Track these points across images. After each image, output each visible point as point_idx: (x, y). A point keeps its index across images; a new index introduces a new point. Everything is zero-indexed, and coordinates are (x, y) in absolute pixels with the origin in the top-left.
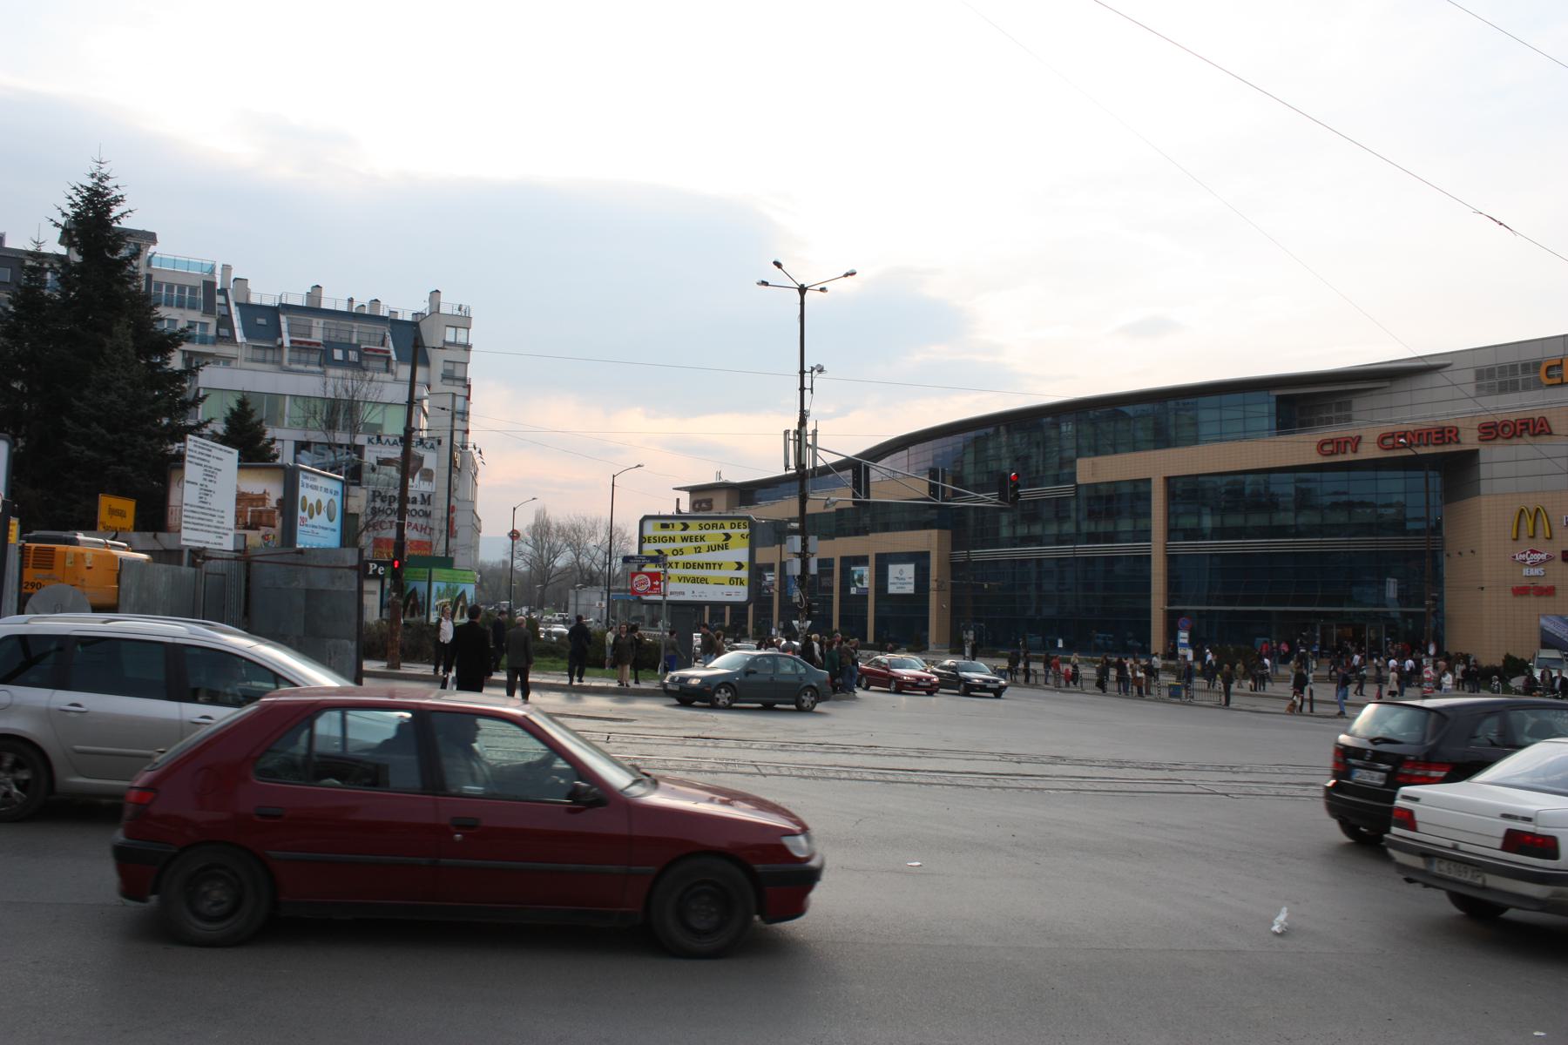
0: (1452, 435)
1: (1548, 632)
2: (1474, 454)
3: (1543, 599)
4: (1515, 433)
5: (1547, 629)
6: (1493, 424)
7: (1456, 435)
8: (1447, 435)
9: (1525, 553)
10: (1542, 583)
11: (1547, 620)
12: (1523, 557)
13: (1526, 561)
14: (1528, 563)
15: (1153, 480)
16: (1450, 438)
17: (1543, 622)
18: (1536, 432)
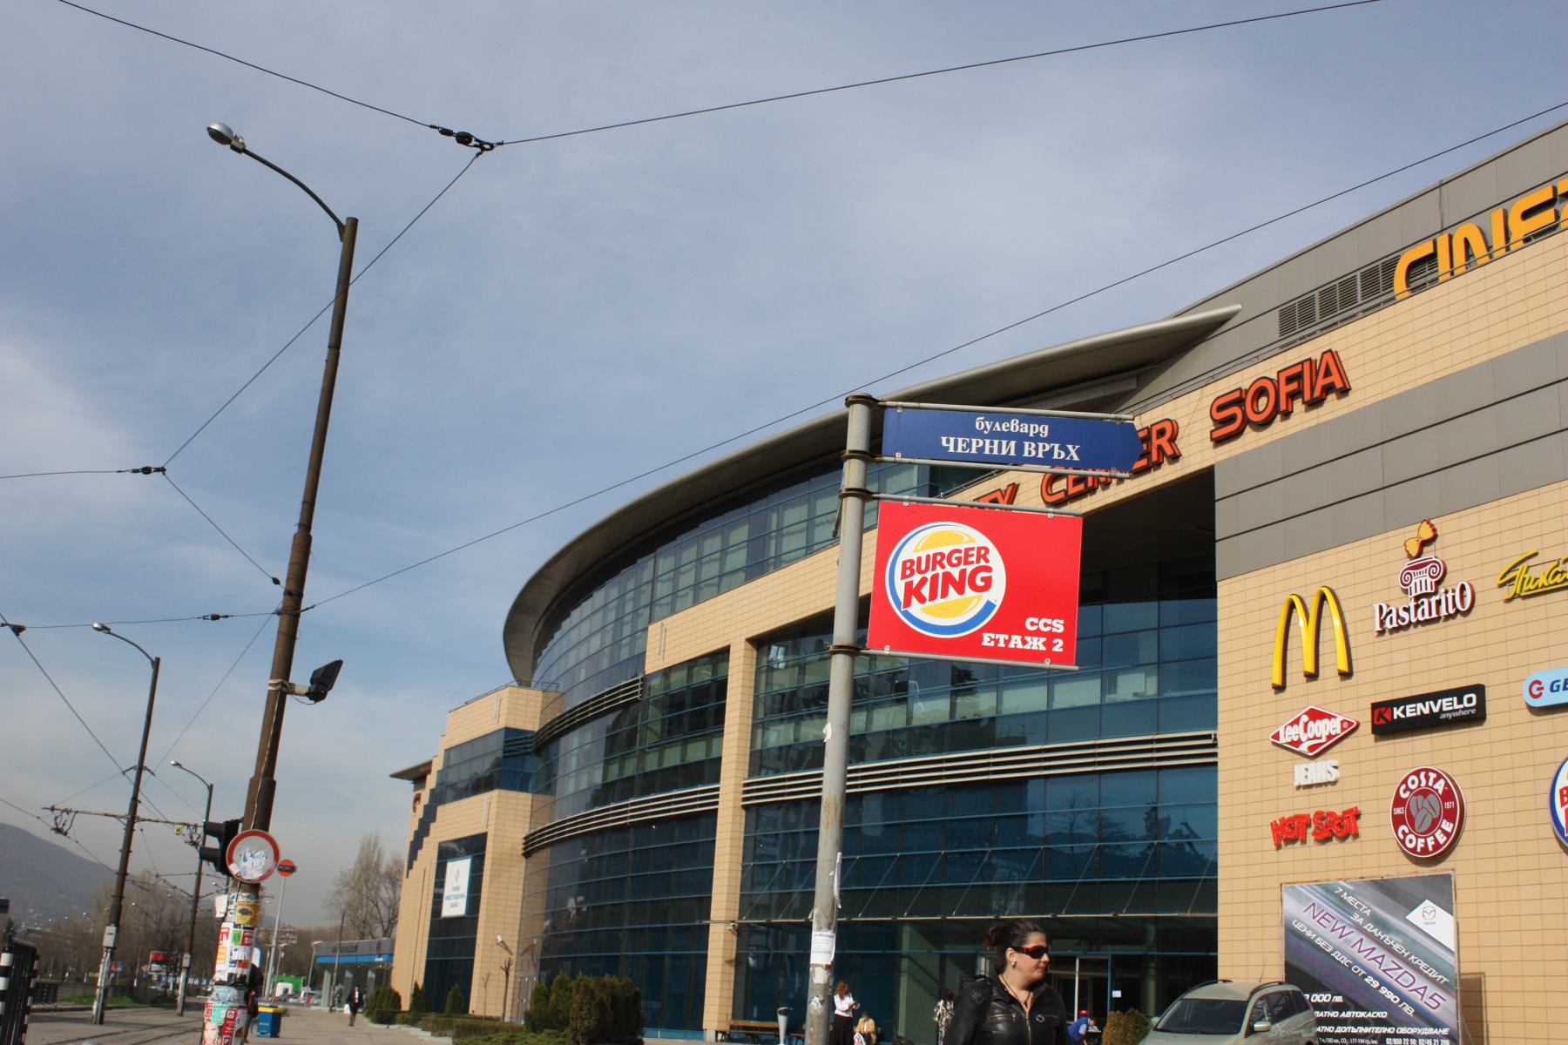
0: (1163, 442)
1: (1300, 936)
2: (1205, 478)
3: (1334, 846)
4: (1276, 410)
5: (1298, 927)
6: (1237, 395)
7: (1172, 440)
8: (1155, 442)
9: (1297, 722)
10: (1335, 804)
11: (1299, 897)
12: (1294, 733)
13: (1298, 743)
14: (1303, 748)
15: (732, 650)
16: (1160, 448)
17: (1292, 907)
18: (1317, 393)
